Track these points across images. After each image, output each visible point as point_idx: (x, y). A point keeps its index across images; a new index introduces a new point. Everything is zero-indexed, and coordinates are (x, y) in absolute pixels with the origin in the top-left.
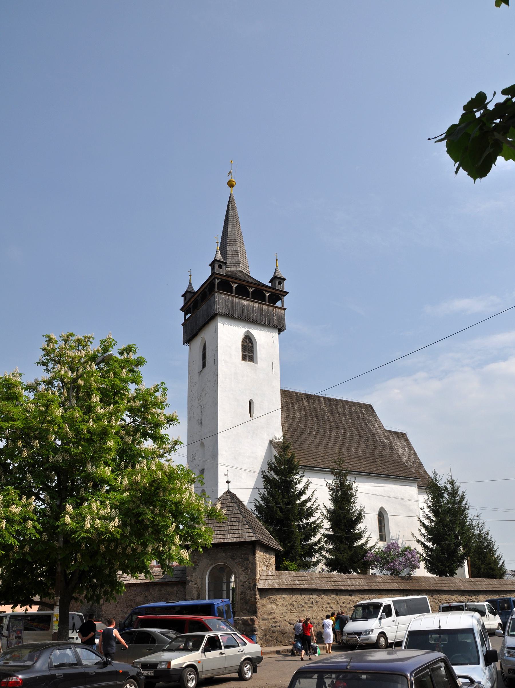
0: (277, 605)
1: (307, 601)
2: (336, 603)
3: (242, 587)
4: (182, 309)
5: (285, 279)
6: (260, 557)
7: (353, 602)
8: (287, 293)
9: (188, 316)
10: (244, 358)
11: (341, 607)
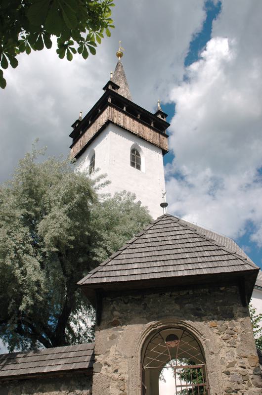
3: (226, 378)
4: (71, 136)
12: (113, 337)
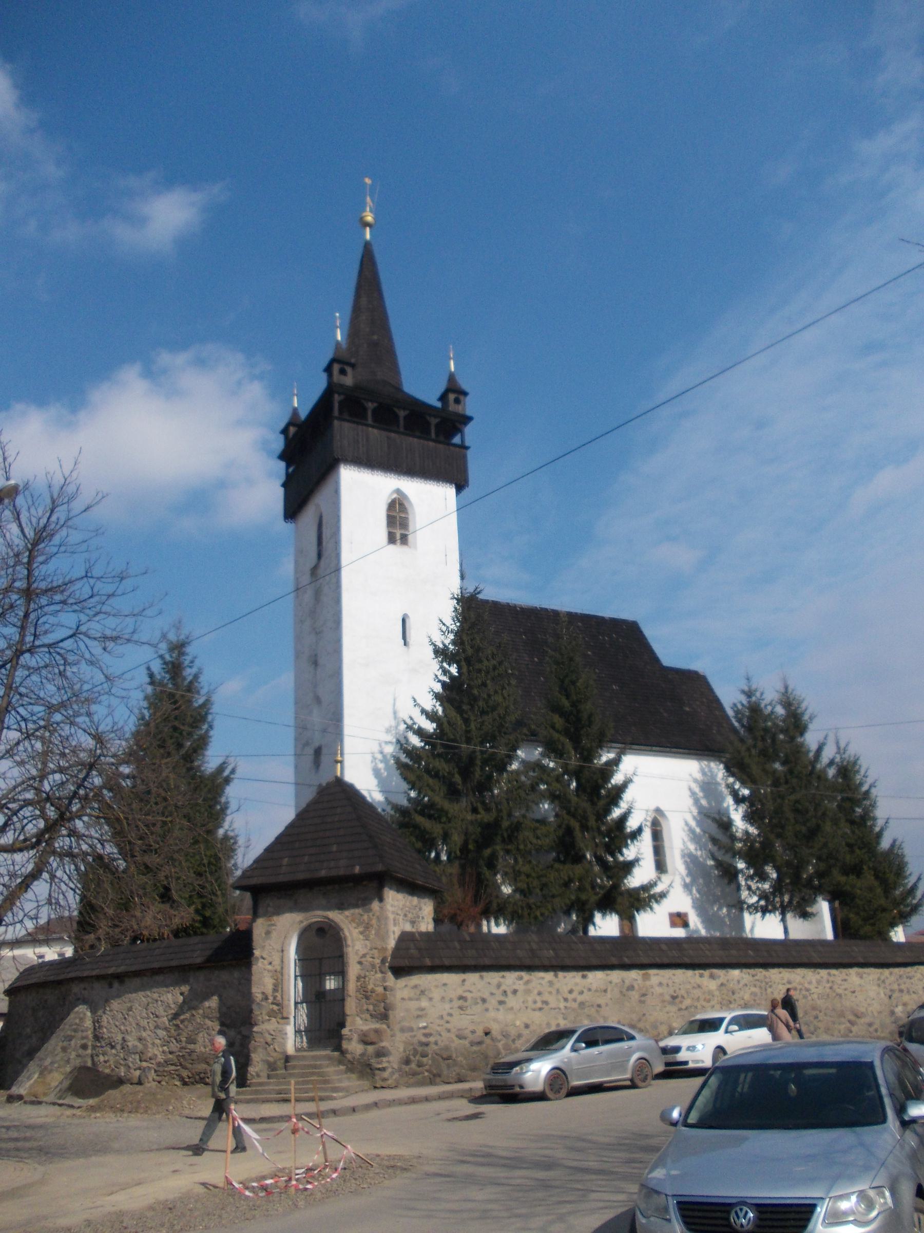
0: (431, 999)
1: (494, 991)
2: (554, 992)
3: (359, 967)
5: (465, 394)
6: (396, 903)
7: (590, 990)
8: (470, 419)
9: (291, 470)
10: (392, 539)
11: (566, 1000)
12: (268, 933)
